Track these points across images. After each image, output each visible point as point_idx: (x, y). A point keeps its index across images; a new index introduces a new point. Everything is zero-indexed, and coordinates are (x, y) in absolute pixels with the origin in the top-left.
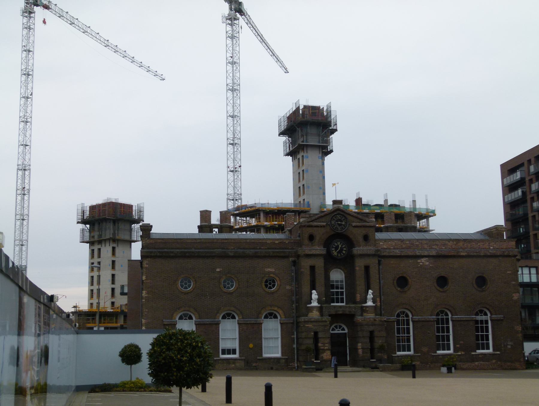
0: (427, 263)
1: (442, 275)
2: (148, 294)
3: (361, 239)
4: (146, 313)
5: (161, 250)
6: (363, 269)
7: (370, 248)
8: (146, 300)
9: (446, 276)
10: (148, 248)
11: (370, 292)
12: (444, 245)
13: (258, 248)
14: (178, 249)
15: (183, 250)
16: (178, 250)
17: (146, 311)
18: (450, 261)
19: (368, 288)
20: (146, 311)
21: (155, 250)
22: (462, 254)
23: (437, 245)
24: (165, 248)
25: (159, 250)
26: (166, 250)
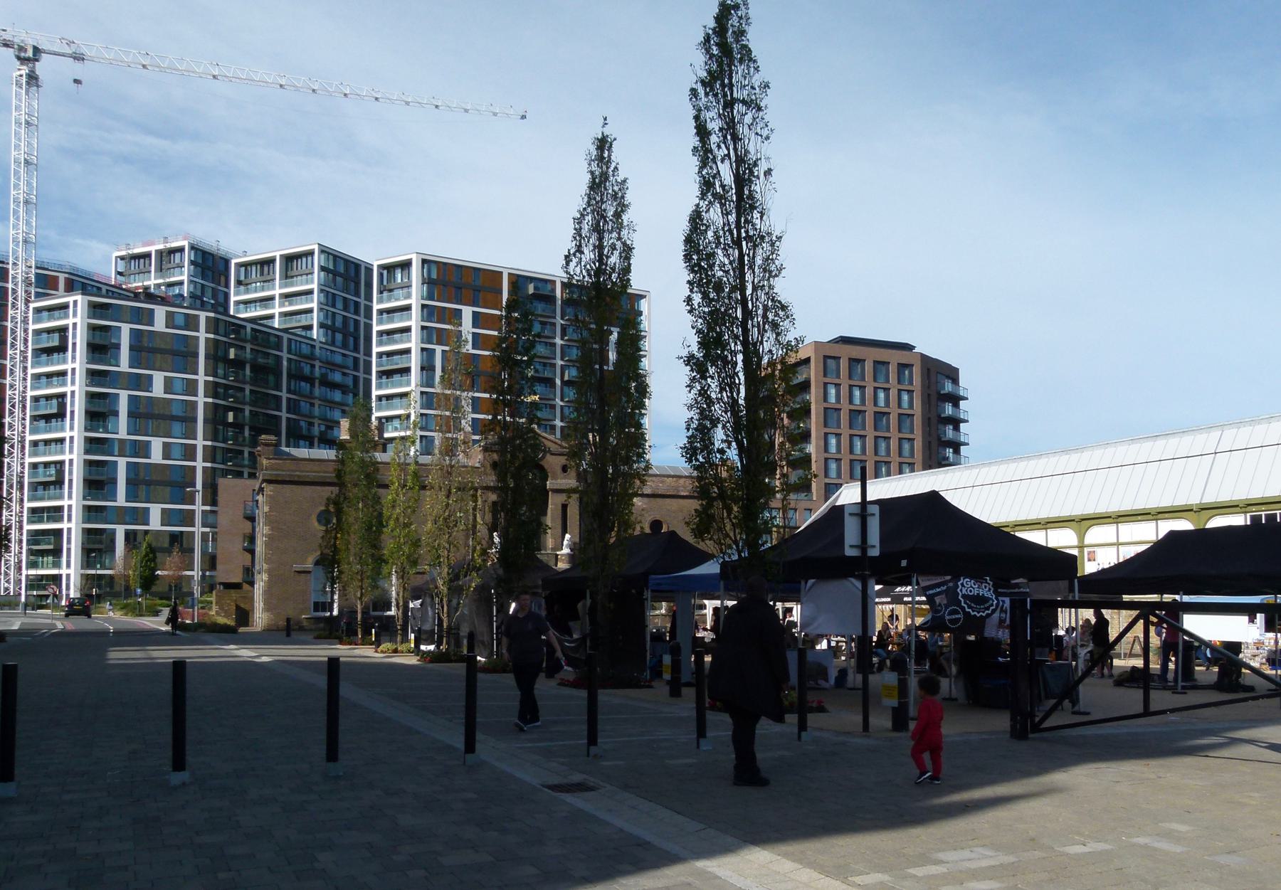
0: (640, 504)
1: (657, 519)
2: (272, 530)
3: (559, 470)
4: (269, 556)
5: (292, 473)
6: (560, 507)
7: (570, 481)
8: (269, 538)
9: (662, 520)
10: (272, 469)
11: (568, 536)
12: (662, 482)
13: (425, 475)
14: (314, 472)
15: (321, 474)
16: (314, 474)
17: (269, 554)
18: (668, 501)
19: (564, 531)
20: (269, 554)
21: (284, 473)
22: (682, 494)
23: (654, 481)
24: (297, 471)
25: (288, 473)
26: (298, 473)
